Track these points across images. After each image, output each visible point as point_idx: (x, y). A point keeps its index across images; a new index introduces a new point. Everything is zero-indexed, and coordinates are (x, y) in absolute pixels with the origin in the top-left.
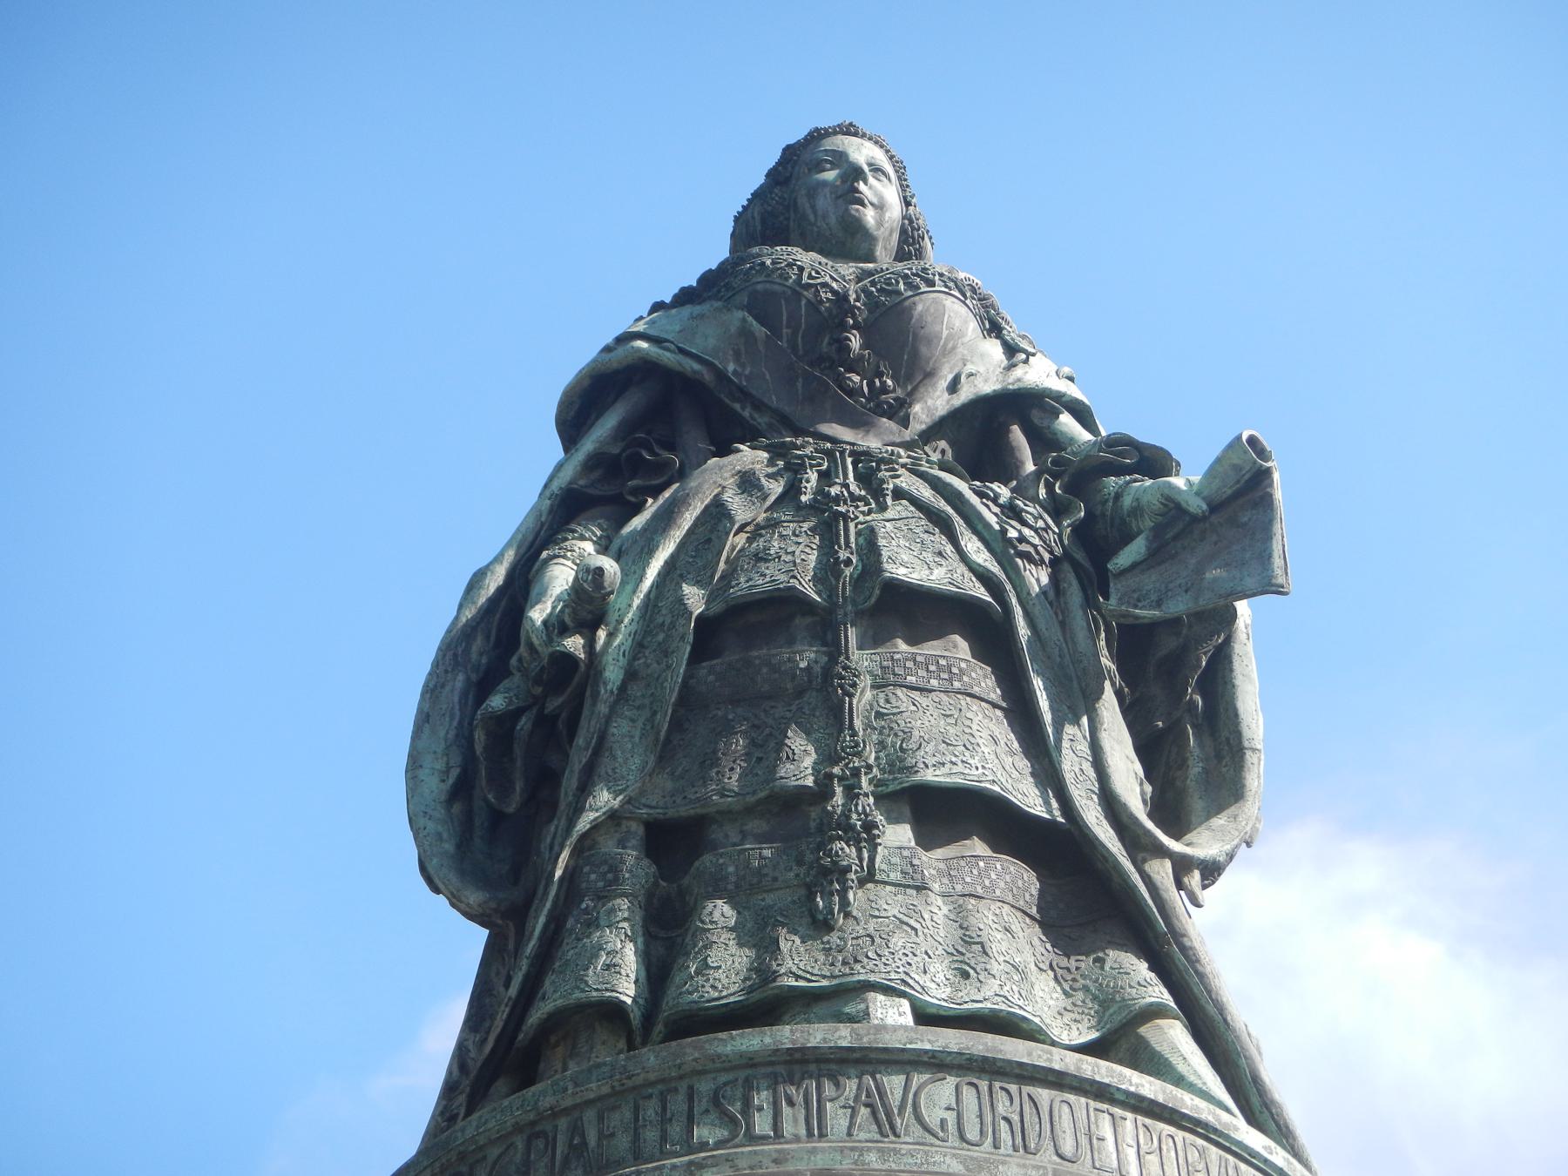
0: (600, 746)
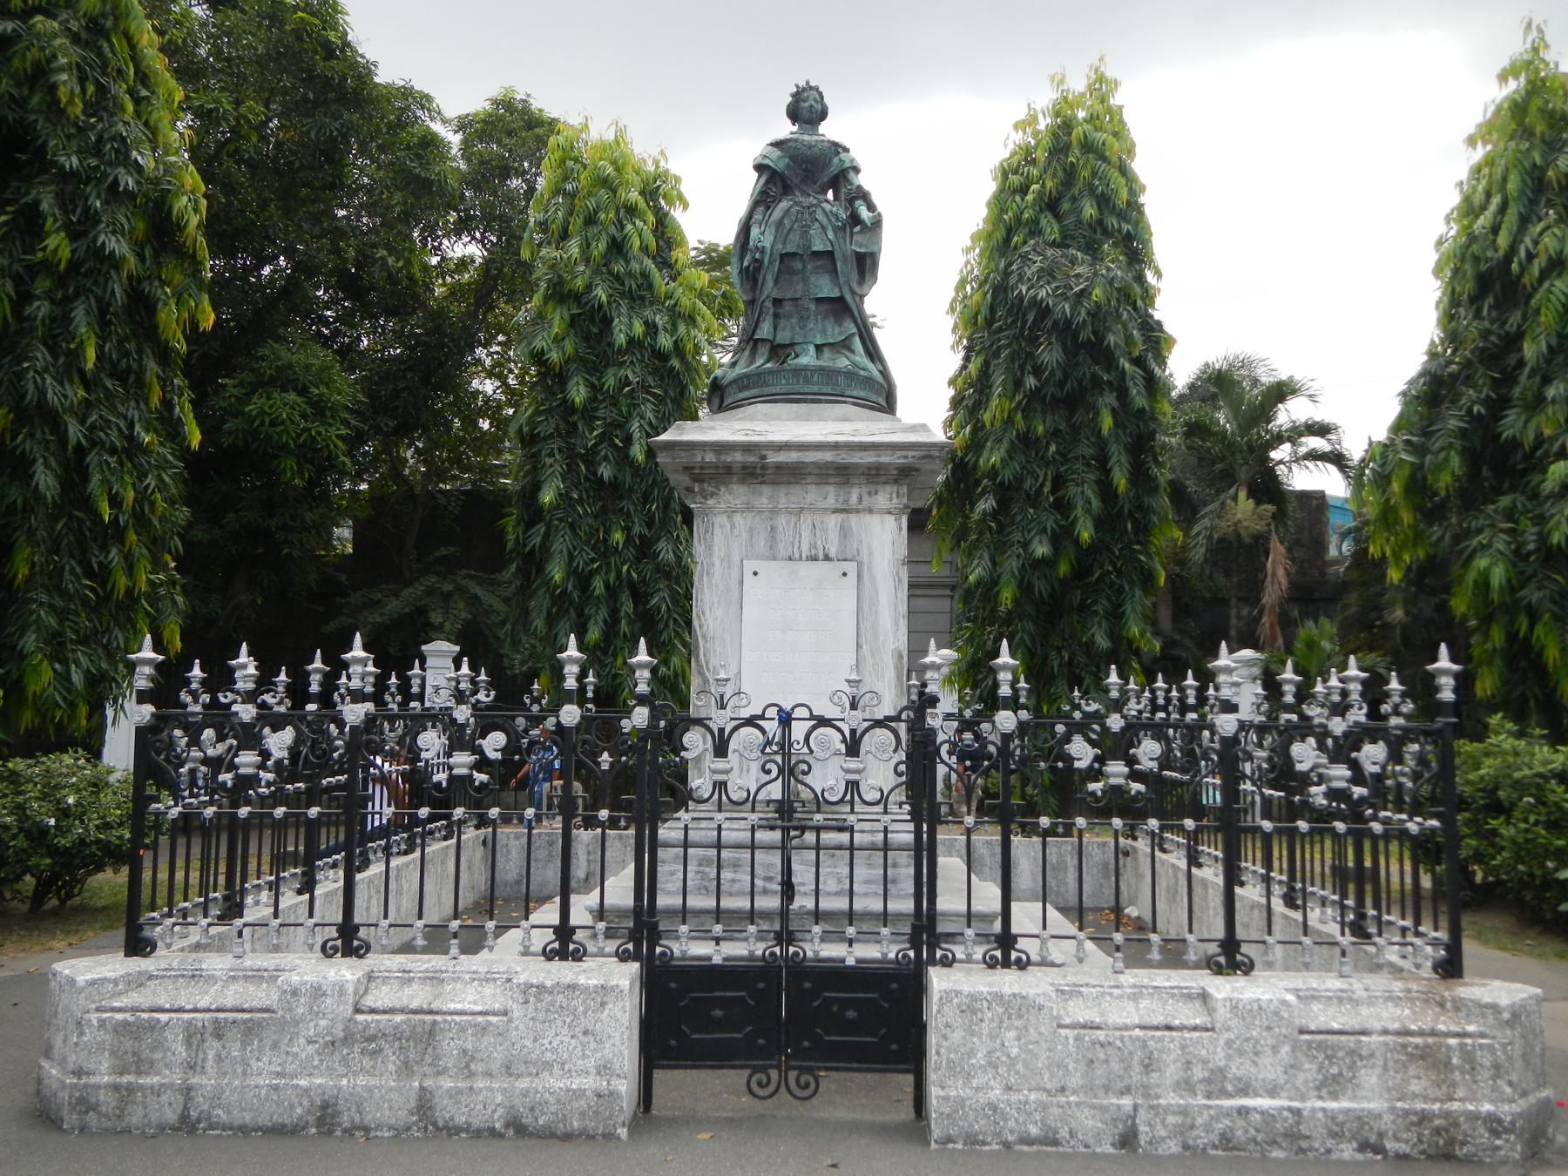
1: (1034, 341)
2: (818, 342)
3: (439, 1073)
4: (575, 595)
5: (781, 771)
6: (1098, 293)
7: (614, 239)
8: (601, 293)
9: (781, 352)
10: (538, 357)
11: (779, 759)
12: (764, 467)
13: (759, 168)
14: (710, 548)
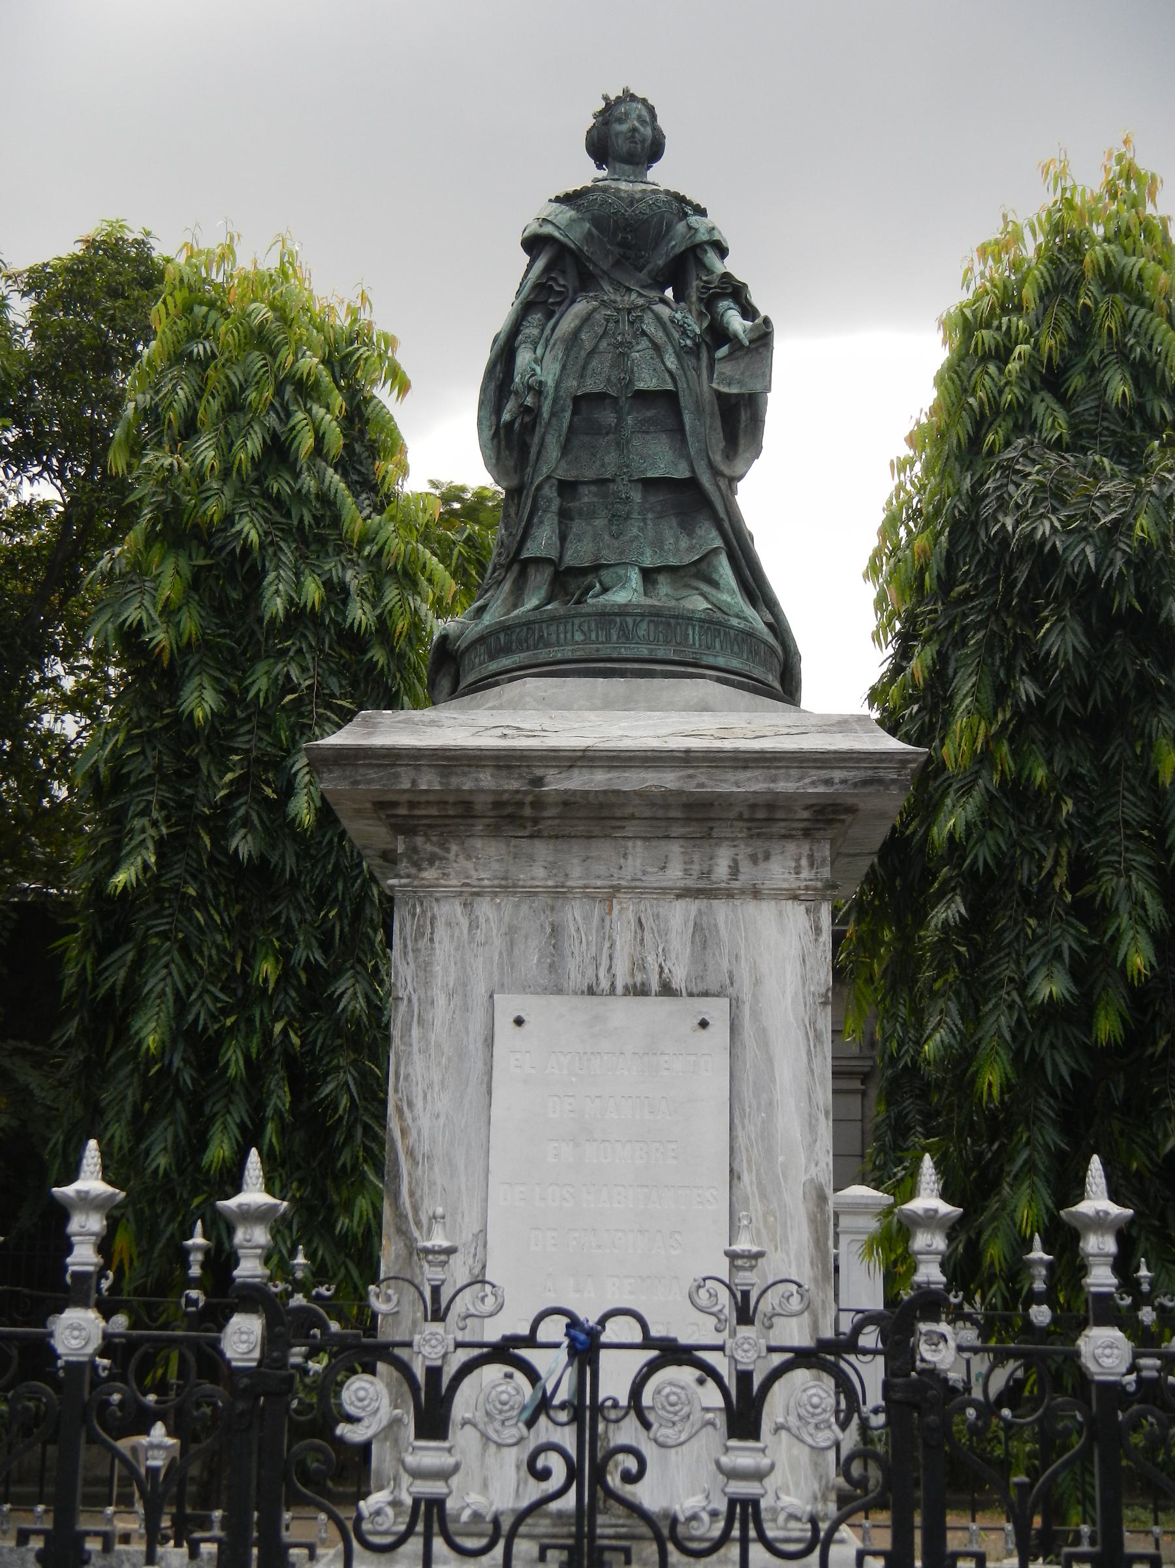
0: (542, 444)
1: (1032, 618)
2: (648, 563)
4: (187, 1077)
5: (574, 1472)
6: (1144, 524)
7: (275, 436)
8: (250, 529)
9: (573, 584)
10: (131, 640)
11: (567, 1438)
12: (538, 804)
13: (533, 244)
14: (425, 968)
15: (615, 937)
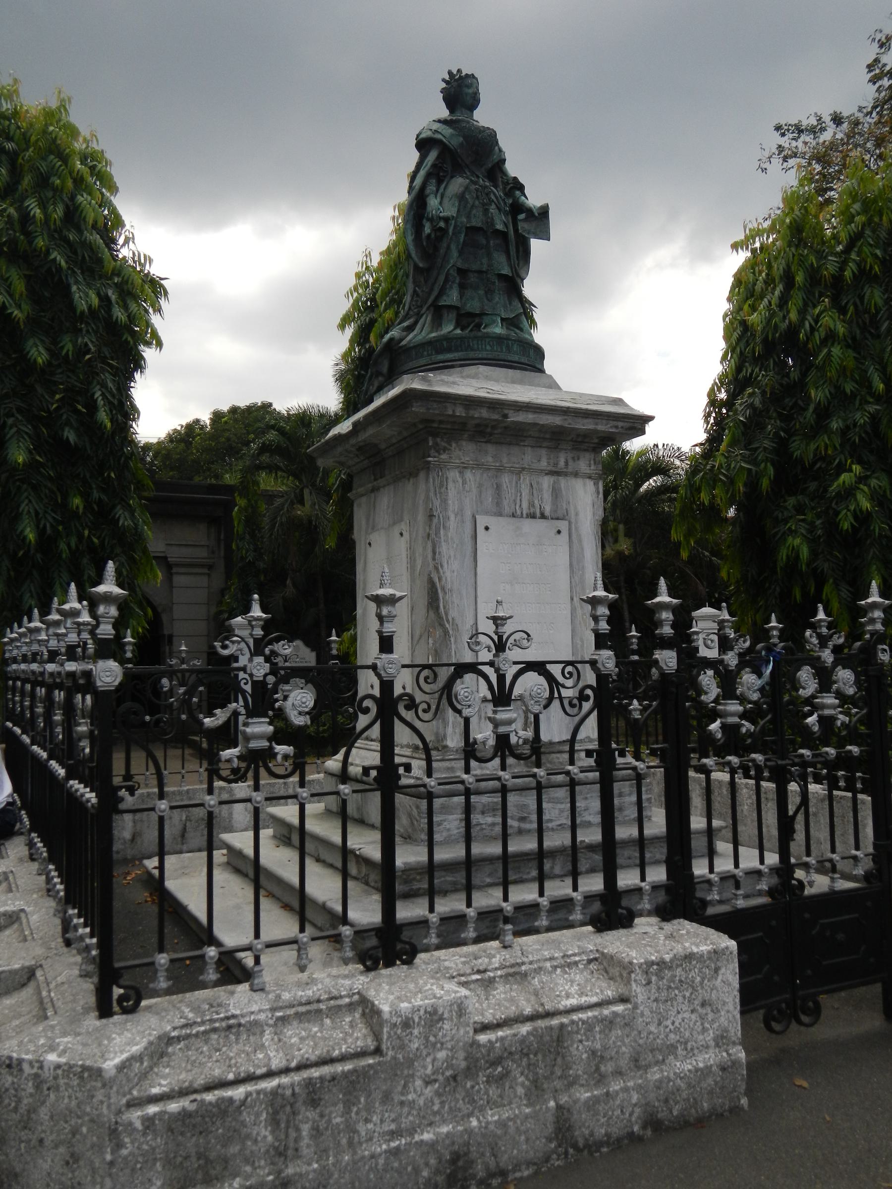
0: (448, 248)
3: (571, 1085)
14: (444, 501)
15: (520, 490)
